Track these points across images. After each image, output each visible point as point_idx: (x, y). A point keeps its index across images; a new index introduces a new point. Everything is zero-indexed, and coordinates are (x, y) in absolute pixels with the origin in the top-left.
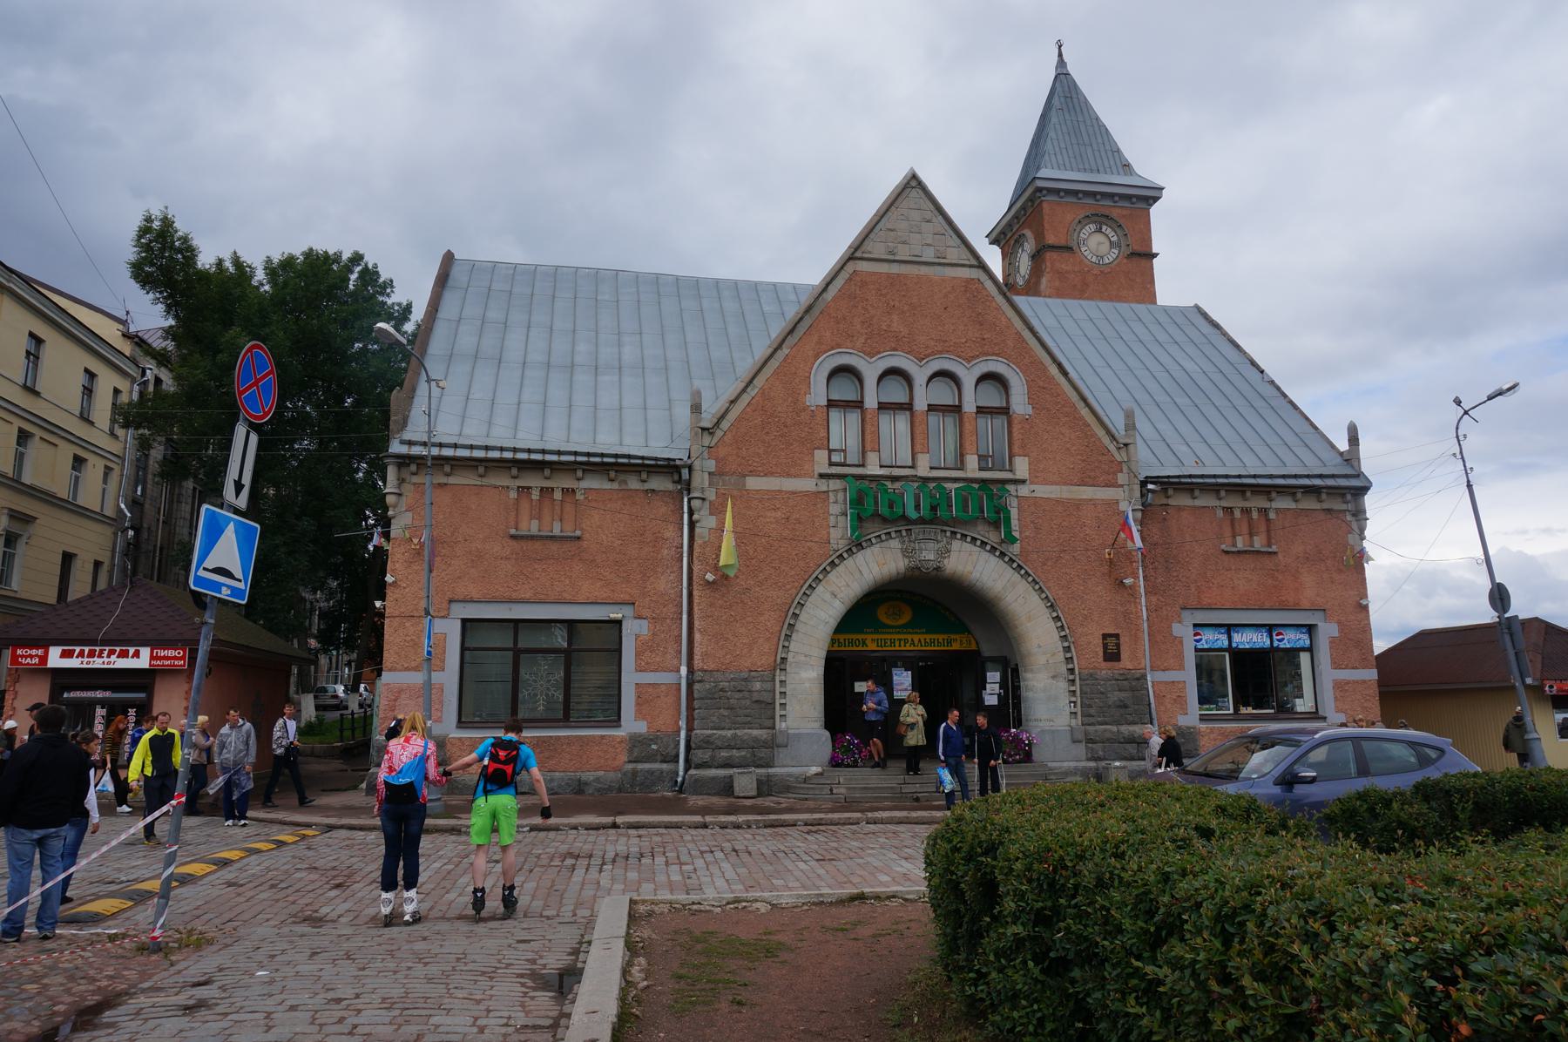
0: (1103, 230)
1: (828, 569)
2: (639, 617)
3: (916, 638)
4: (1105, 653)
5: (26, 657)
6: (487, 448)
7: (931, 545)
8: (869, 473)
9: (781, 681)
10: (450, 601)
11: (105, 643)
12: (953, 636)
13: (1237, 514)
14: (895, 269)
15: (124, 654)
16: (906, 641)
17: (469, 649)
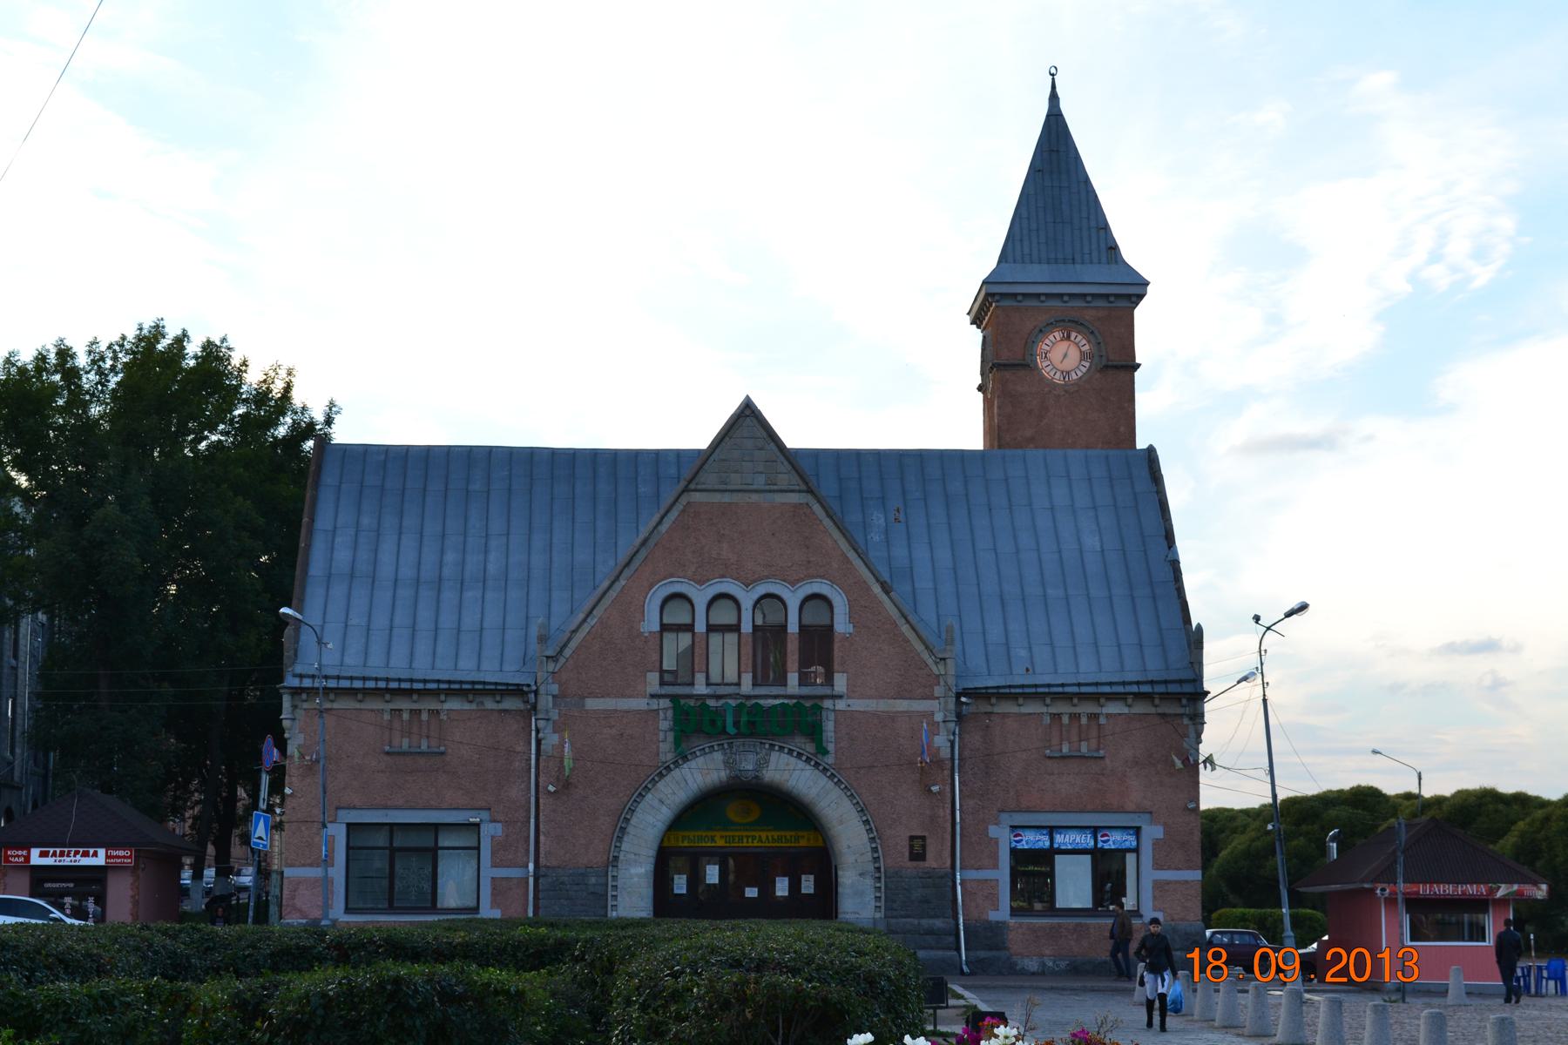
0: (1072, 338)
1: (656, 779)
2: (494, 821)
3: (764, 835)
4: (911, 853)
5: (15, 857)
6: (364, 679)
7: (751, 757)
8: (695, 692)
9: (613, 876)
10: (338, 808)
12: (800, 834)
13: (1065, 720)
14: (727, 498)
15: (86, 854)
16: (754, 838)
17: (353, 848)
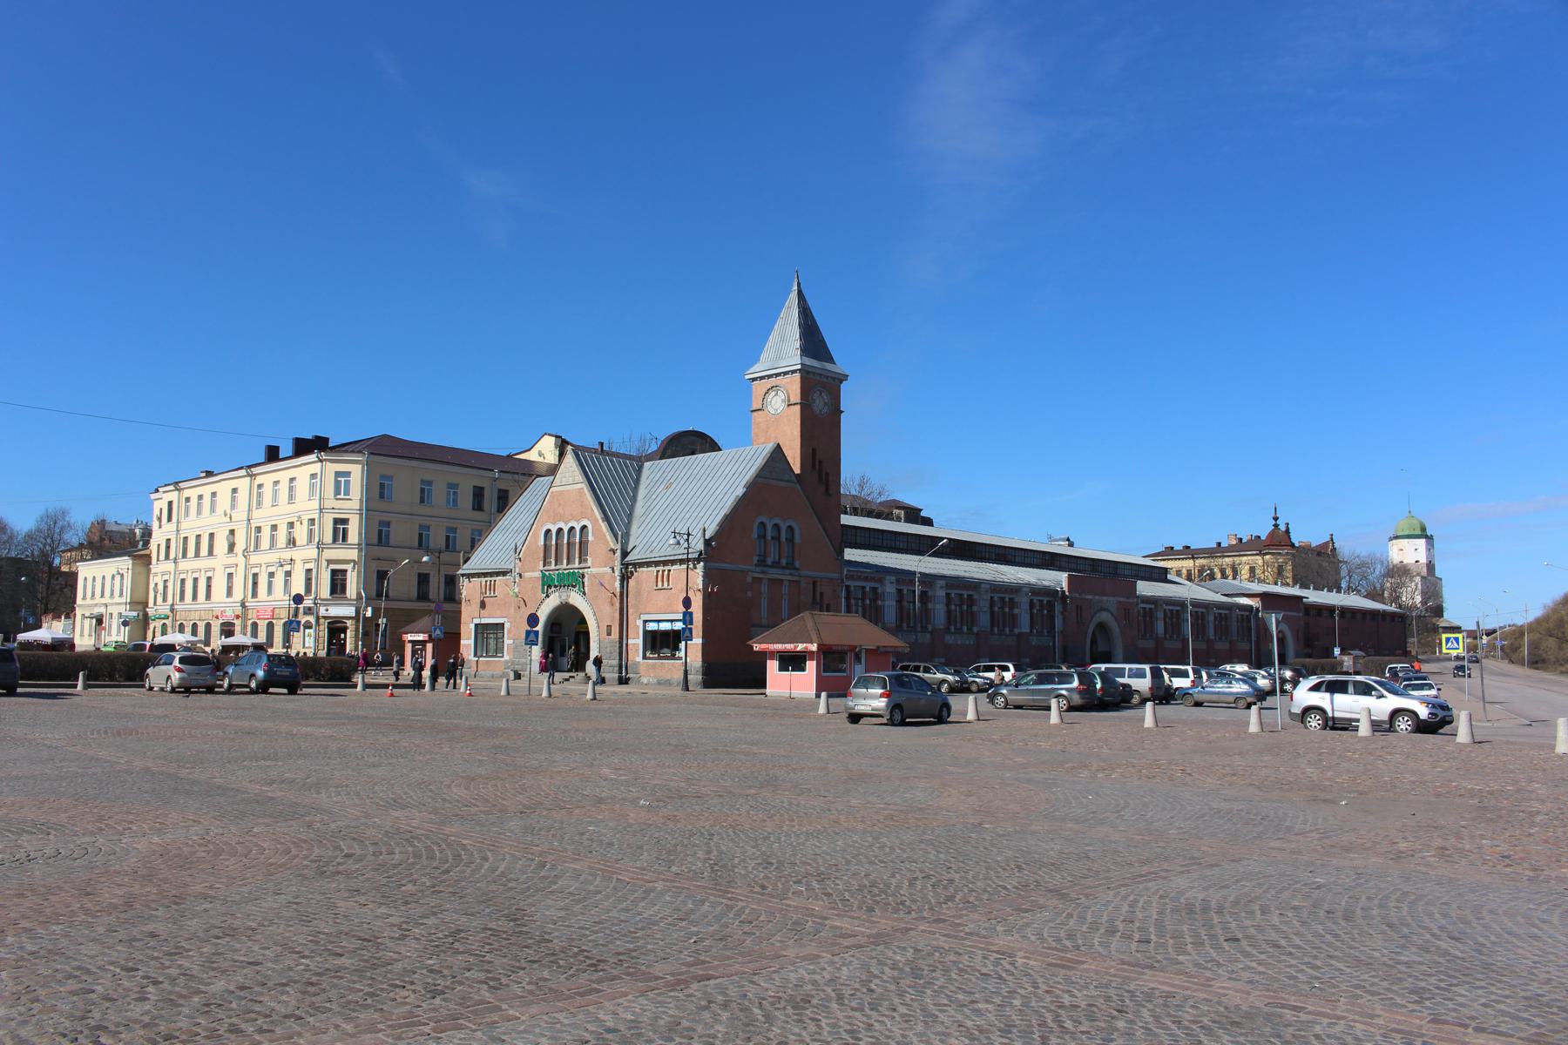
11: (416, 633)
